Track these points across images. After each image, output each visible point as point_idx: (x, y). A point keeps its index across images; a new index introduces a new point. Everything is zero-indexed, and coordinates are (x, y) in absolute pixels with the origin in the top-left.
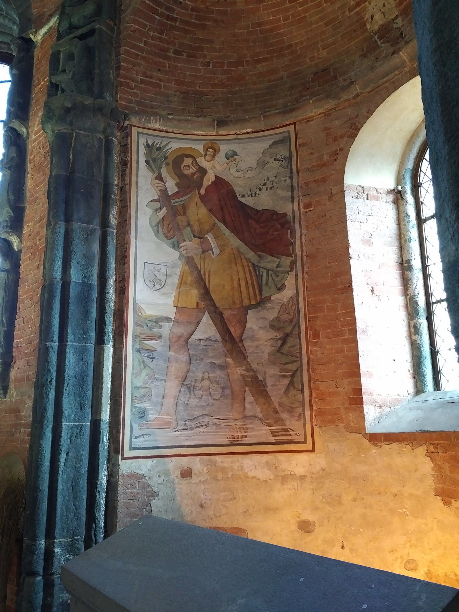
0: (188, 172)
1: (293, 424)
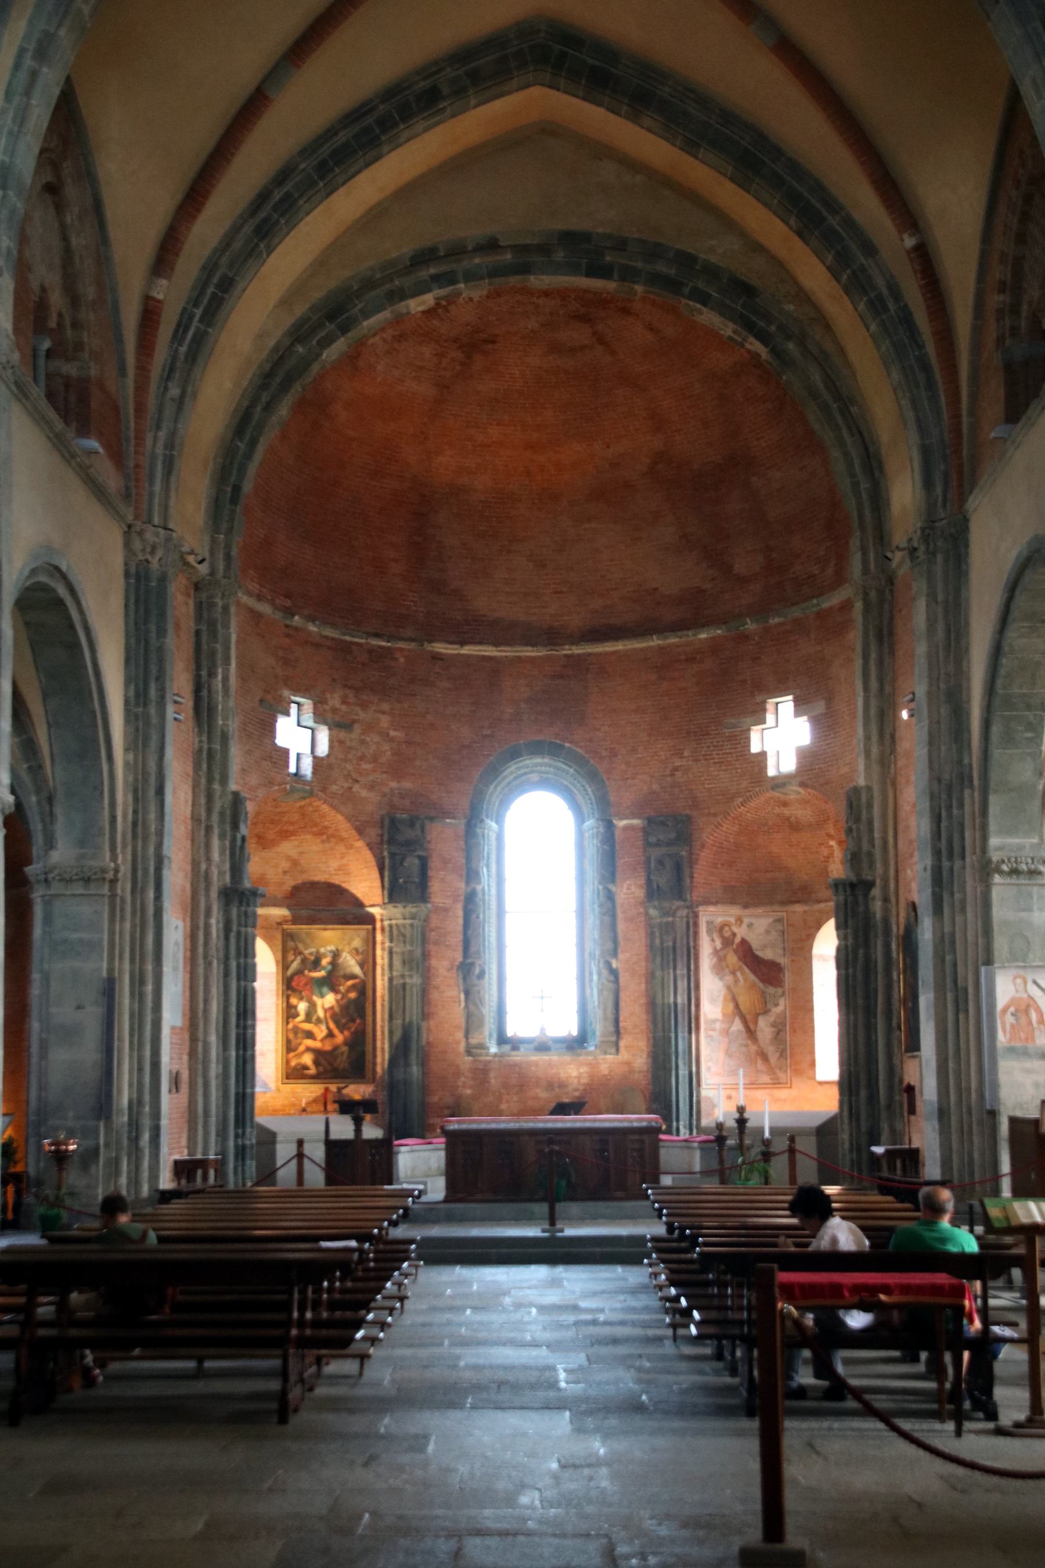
0: (727, 934)
1: (782, 1076)
